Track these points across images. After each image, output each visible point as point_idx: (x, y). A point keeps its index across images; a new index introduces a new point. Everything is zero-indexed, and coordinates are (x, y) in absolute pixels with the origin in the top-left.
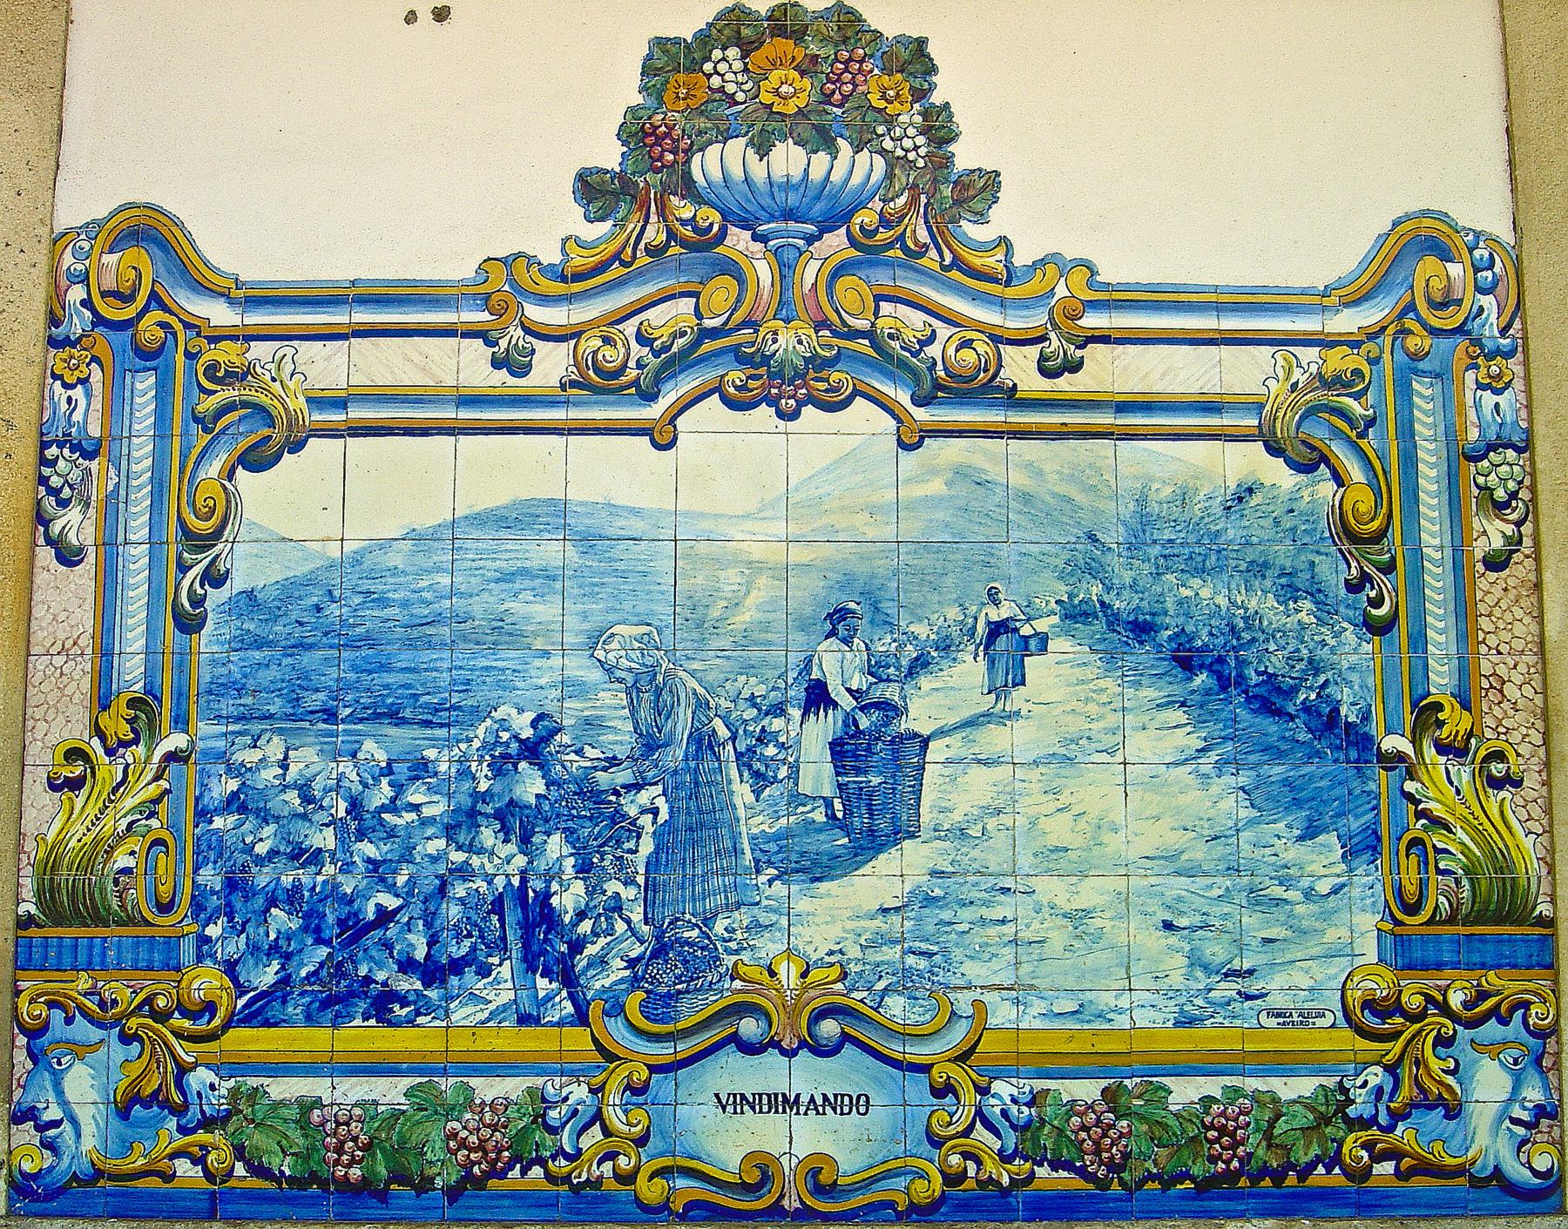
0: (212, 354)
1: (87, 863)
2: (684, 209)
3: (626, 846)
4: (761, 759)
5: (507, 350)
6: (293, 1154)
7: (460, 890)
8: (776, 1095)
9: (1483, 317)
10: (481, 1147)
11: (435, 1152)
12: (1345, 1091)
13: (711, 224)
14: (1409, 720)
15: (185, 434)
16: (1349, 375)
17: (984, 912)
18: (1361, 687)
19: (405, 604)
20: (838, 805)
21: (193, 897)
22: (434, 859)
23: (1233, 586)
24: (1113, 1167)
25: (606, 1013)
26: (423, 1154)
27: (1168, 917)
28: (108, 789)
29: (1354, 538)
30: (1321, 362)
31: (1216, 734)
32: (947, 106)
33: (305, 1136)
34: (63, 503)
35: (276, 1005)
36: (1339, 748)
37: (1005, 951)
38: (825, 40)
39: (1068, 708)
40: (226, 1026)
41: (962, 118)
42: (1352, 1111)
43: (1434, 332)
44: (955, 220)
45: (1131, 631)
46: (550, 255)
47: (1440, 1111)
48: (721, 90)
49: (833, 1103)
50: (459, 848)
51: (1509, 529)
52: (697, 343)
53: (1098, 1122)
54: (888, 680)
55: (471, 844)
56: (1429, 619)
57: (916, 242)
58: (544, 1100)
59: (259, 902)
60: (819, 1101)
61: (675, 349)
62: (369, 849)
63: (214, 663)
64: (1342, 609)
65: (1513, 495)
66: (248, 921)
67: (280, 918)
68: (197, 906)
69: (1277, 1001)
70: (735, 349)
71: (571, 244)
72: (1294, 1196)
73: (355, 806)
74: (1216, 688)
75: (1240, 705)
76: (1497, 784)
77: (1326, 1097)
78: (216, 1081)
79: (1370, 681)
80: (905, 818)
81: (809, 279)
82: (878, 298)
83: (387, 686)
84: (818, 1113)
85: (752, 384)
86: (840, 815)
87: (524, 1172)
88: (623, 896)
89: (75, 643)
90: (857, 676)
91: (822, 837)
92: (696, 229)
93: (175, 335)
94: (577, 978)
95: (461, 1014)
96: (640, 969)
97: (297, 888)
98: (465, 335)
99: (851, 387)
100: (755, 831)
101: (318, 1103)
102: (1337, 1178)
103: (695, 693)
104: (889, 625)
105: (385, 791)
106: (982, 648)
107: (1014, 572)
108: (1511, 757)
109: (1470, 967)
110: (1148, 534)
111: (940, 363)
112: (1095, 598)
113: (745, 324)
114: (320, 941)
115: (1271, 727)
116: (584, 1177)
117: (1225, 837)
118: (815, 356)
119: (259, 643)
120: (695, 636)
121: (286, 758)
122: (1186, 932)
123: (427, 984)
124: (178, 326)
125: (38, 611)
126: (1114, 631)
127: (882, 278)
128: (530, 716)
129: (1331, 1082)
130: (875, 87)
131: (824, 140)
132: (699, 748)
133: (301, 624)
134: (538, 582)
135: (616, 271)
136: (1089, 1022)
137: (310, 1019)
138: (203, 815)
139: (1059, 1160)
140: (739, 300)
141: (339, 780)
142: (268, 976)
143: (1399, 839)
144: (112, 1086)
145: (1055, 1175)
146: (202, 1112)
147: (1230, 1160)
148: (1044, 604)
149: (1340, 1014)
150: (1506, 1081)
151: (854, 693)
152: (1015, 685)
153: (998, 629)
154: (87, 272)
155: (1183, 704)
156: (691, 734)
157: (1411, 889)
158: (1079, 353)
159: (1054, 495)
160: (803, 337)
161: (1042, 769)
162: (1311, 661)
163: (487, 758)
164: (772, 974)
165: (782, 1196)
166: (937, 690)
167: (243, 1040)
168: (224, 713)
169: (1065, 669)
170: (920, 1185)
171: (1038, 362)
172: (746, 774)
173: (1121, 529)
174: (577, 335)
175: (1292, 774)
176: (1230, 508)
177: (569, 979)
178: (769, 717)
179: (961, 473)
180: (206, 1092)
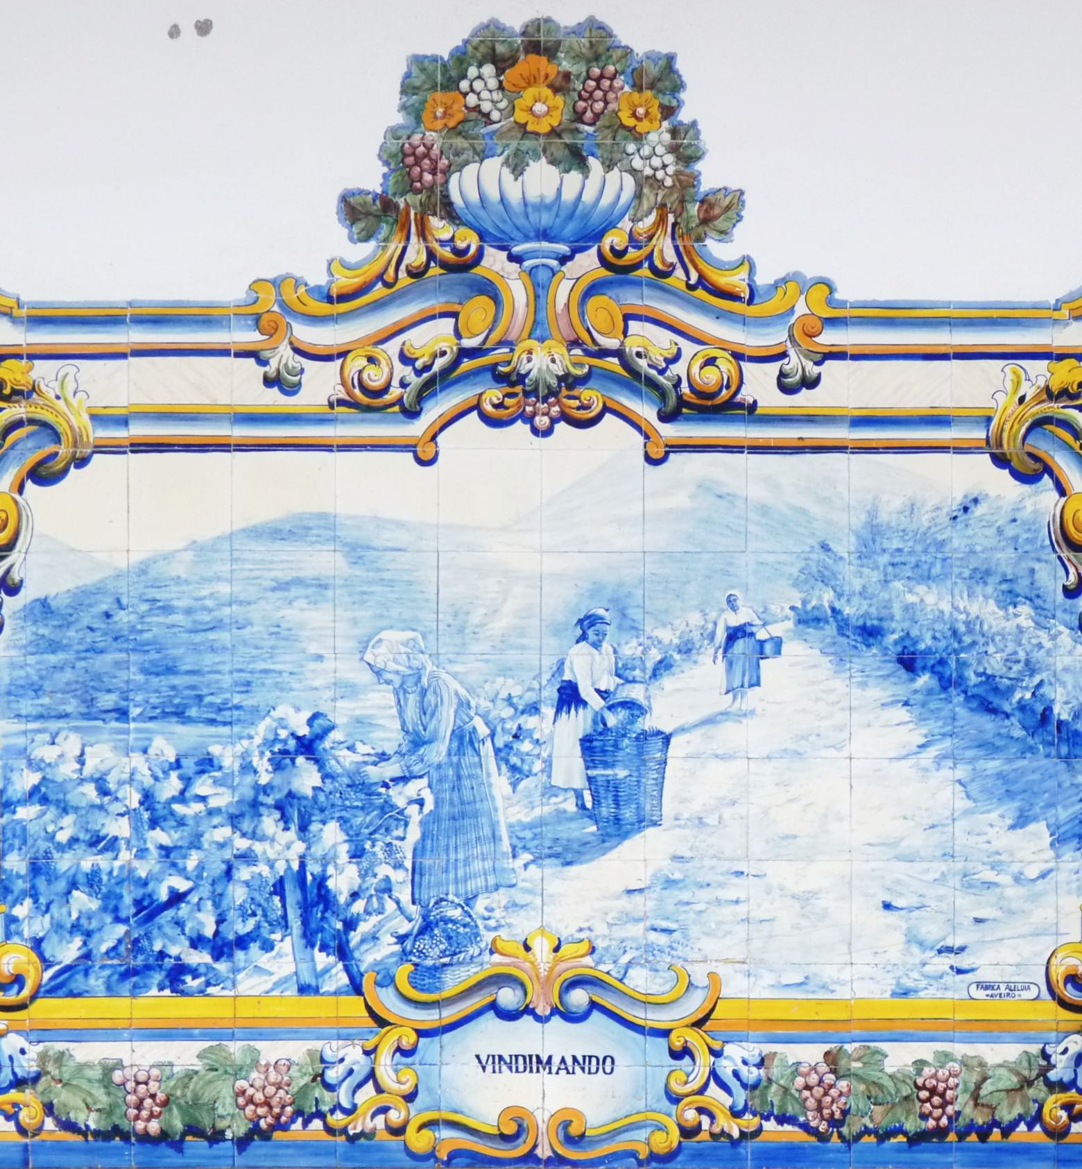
2: (440, 228)
4: (518, 754)
5: (278, 371)
6: (98, 1110)
7: (244, 873)
8: (531, 1057)
10: (267, 1103)
11: (226, 1107)
12: (1045, 1055)
16: (1075, 387)
18: (1074, 687)
19: (188, 611)
22: (222, 846)
23: (956, 591)
25: (378, 984)
26: (214, 1109)
30: (1048, 375)
31: (936, 731)
32: (694, 124)
33: (109, 1094)
35: (80, 977)
36: (1051, 744)
38: (578, 57)
40: (34, 997)
41: (708, 138)
42: (1053, 1075)
44: (699, 239)
45: (859, 635)
46: (318, 278)
48: (477, 108)
49: (583, 1063)
50: (244, 835)
52: (456, 363)
53: (821, 1081)
54: (634, 681)
55: (254, 832)
57: (663, 261)
58: (322, 1060)
59: (61, 885)
60: (569, 1061)
62: (159, 836)
64: (1059, 614)
67: (82, 901)
69: (985, 975)
70: (493, 368)
72: (999, 1150)
73: (147, 798)
75: (959, 704)
77: (1029, 1062)
78: (26, 1045)
80: (648, 807)
82: (627, 318)
83: (173, 688)
84: (568, 1073)
85: (508, 401)
86: (589, 805)
87: (306, 1123)
88: (393, 879)
91: (574, 825)
92: (456, 251)
94: (352, 952)
95: (248, 984)
96: (408, 944)
98: (238, 355)
99: (601, 405)
100: (512, 820)
101: (119, 1065)
103: (457, 694)
104: (635, 629)
105: (173, 785)
106: (721, 651)
110: (878, 543)
113: (502, 343)
114: (118, 920)
115: (988, 724)
116: (358, 1130)
117: (942, 825)
119: (54, 647)
120: (457, 640)
121: (82, 754)
122: (903, 913)
123: (217, 956)
126: (843, 635)
127: (633, 299)
128: (307, 714)
129: (1035, 1049)
131: (576, 159)
132: (461, 744)
133: (91, 629)
134: (311, 590)
135: (379, 291)
136: (813, 992)
137: (110, 991)
139: (784, 1115)
140: (495, 321)
141: (132, 774)
142: (69, 951)
145: (780, 1128)
146: (14, 1074)
148: (778, 611)
149: (1044, 988)
151: (603, 694)
152: (751, 686)
153: (734, 635)
155: (906, 704)
156: (453, 731)
158: (816, 370)
160: (556, 356)
161: (774, 763)
162: (1027, 663)
164: (527, 948)
165: (535, 1146)
166: (679, 690)
167: (49, 1009)
168: (24, 713)
171: (779, 379)
172: (504, 768)
173: (853, 539)
174: (343, 354)
175: (1005, 767)
176: (955, 518)
177: (343, 953)
178: (525, 716)
179: (703, 487)
180: (17, 1056)
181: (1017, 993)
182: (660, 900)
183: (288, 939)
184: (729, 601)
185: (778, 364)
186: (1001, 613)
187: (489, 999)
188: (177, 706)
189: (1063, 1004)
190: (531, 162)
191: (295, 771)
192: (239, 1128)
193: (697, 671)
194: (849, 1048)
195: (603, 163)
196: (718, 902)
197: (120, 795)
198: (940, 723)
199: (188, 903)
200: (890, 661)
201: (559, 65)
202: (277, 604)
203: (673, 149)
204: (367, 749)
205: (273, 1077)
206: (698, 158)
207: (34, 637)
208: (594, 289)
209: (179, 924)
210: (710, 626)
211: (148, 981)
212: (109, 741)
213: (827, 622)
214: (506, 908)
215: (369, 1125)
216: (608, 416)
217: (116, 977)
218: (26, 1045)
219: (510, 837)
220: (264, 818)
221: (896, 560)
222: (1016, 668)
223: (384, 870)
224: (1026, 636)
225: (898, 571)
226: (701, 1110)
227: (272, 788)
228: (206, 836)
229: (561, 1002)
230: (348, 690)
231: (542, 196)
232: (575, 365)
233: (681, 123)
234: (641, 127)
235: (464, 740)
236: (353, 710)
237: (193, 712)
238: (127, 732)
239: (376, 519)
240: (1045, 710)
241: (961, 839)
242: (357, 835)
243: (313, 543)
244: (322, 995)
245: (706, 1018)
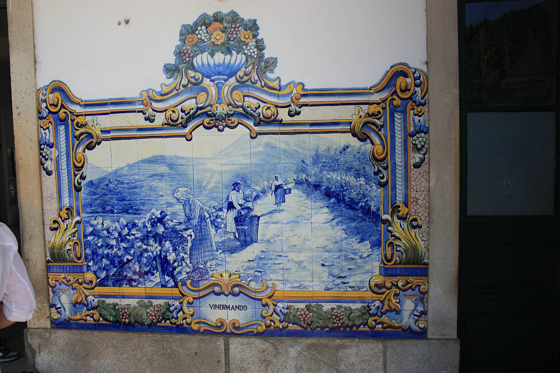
0: (78, 120)
1: (61, 248)
2: (191, 73)
3: (185, 244)
6: (113, 316)
8: (224, 305)
9: (417, 94)
10: (155, 316)
11: (145, 316)
12: (369, 307)
13: (199, 78)
14: (390, 210)
15: (73, 140)
16: (376, 113)
18: (377, 201)
19: (128, 184)
20: (237, 234)
21: (85, 256)
22: (139, 247)
23: (342, 174)
24: (308, 324)
25: (182, 285)
27: (323, 263)
28: (63, 230)
30: (368, 109)
31: (337, 215)
33: (115, 312)
34: (46, 160)
35: (106, 282)
36: (370, 218)
37: (280, 271)
38: (228, 22)
39: (296, 208)
40: (95, 286)
41: (266, 43)
42: (371, 312)
43: (402, 99)
44: (264, 73)
45: (314, 187)
46: (158, 89)
47: (395, 313)
48: (201, 39)
49: (238, 307)
50: (145, 245)
51: (421, 156)
53: (305, 314)
54: (249, 201)
56: (397, 182)
57: (254, 79)
58: (169, 305)
59: (100, 257)
60: (235, 307)
61: (191, 113)
62: (123, 245)
63: (85, 199)
64: (372, 180)
65: (423, 146)
66: (98, 261)
68: (86, 258)
70: (206, 113)
73: (120, 234)
74: (337, 202)
75: (343, 207)
76: (414, 227)
77: (364, 308)
78: (94, 299)
79: (380, 200)
80: (254, 237)
81: (225, 92)
82: (244, 96)
83: (125, 204)
84: (234, 310)
85: (211, 122)
86: (237, 237)
87: (165, 321)
88: (184, 257)
89: (53, 195)
90: (241, 200)
91: (233, 242)
92: (196, 80)
93: (68, 115)
94: (175, 276)
97: (108, 254)
98: (138, 112)
100: (216, 241)
101: (117, 304)
102: (366, 329)
103: (200, 206)
104: (249, 187)
105: (126, 231)
106: (273, 192)
107: (282, 172)
108: (419, 220)
109: (404, 276)
110: (318, 160)
111: (261, 114)
112: (304, 178)
114: (114, 267)
115: (352, 213)
116: (179, 323)
117: (339, 242)
118: (228, 114)
119: (95, 194)
120: (199, 190)
121: (103, 222)
122: (328, 267)
124: (69, 113)
125: (44, 187)
126: (309, 187)
127: (245, 91)
128: (160, 212)
130: (243, 34)
131: (229, 51)
132: (201, 220)
134: (159, 177)
136: (302, 289)
137: (114, 285)
138: (85, 236)
140: (207, 99)
141: (116, 228)
142: (103, 275)
143: (386, 242)
144: (71, 300)
145: (293, 326)
146: (92, 306)
147: (339, 323)
148: (290, 180)
149: (368, 288)
153: (278, 187)
154: (46, 99)
155: (328, 207)
156: (199, 216)
157: (389, 256)
158: (299, 109)
159: (293, 150)
160: (224, 108)
161: (290, 224)
162: (363, 194)
163: (150, 222)
164: (222, 276)
165: (226, 329)
166: (262, 204)
168: (88, 211)
169: (296, 198)
170: (260, 328)
171: (288, 113)
172: (213, 226)
173: (311, 159)
174: (166, 111)
175: (357, 225)
176: (341, 152)
177: (173, 277)
179: (267, 145)
180: (92, 301)
181: (361, 289)
182: (258, 263)
183: (158, 272)
184: (275, 178)
186: (355, 180)
187: (213, 289)
188: (126, 209)
190: (216, 53)
191: (157, 227)
193: (267, 198)
195: (236, 52)
196: (275, 264)
197: (113, 233)
198: (338, 212)
199: (132, 262)
200: (323, 195)
201: (223, 25)
202: (151, 181)
203: (257, 47)
204: (176, 221)
206: (263, 49)
207: (89, 191)
208: (233, 90)
209: (130, 268)
210: (270, 185)
211: (123, 283)
212: (109, 219)
213: (304, 184)
214: (215, 265)
215: (182, 322)
217: (115, 282)
218: (94, 299)
219: (216, 246)
220: (150, 240)
221: (324, 165)
222: (360, 196)
223: (182, 254)
224: (363, 186)
225: (325, 168)
226: (271, 321)
227: (152, 232)
228: (135, 245)
229: (232, 291)
230: (170, 205)
232: (230, 111)
233: (258, 39)
235: (202, 219)
236: (172, 210)
238: (114, 217)
239: (176, 156)
240: (368, 208)
241: (344, 246)
242: (175, 245)
243: (159, 164)
244: (168, 287)
245: (272, 296)
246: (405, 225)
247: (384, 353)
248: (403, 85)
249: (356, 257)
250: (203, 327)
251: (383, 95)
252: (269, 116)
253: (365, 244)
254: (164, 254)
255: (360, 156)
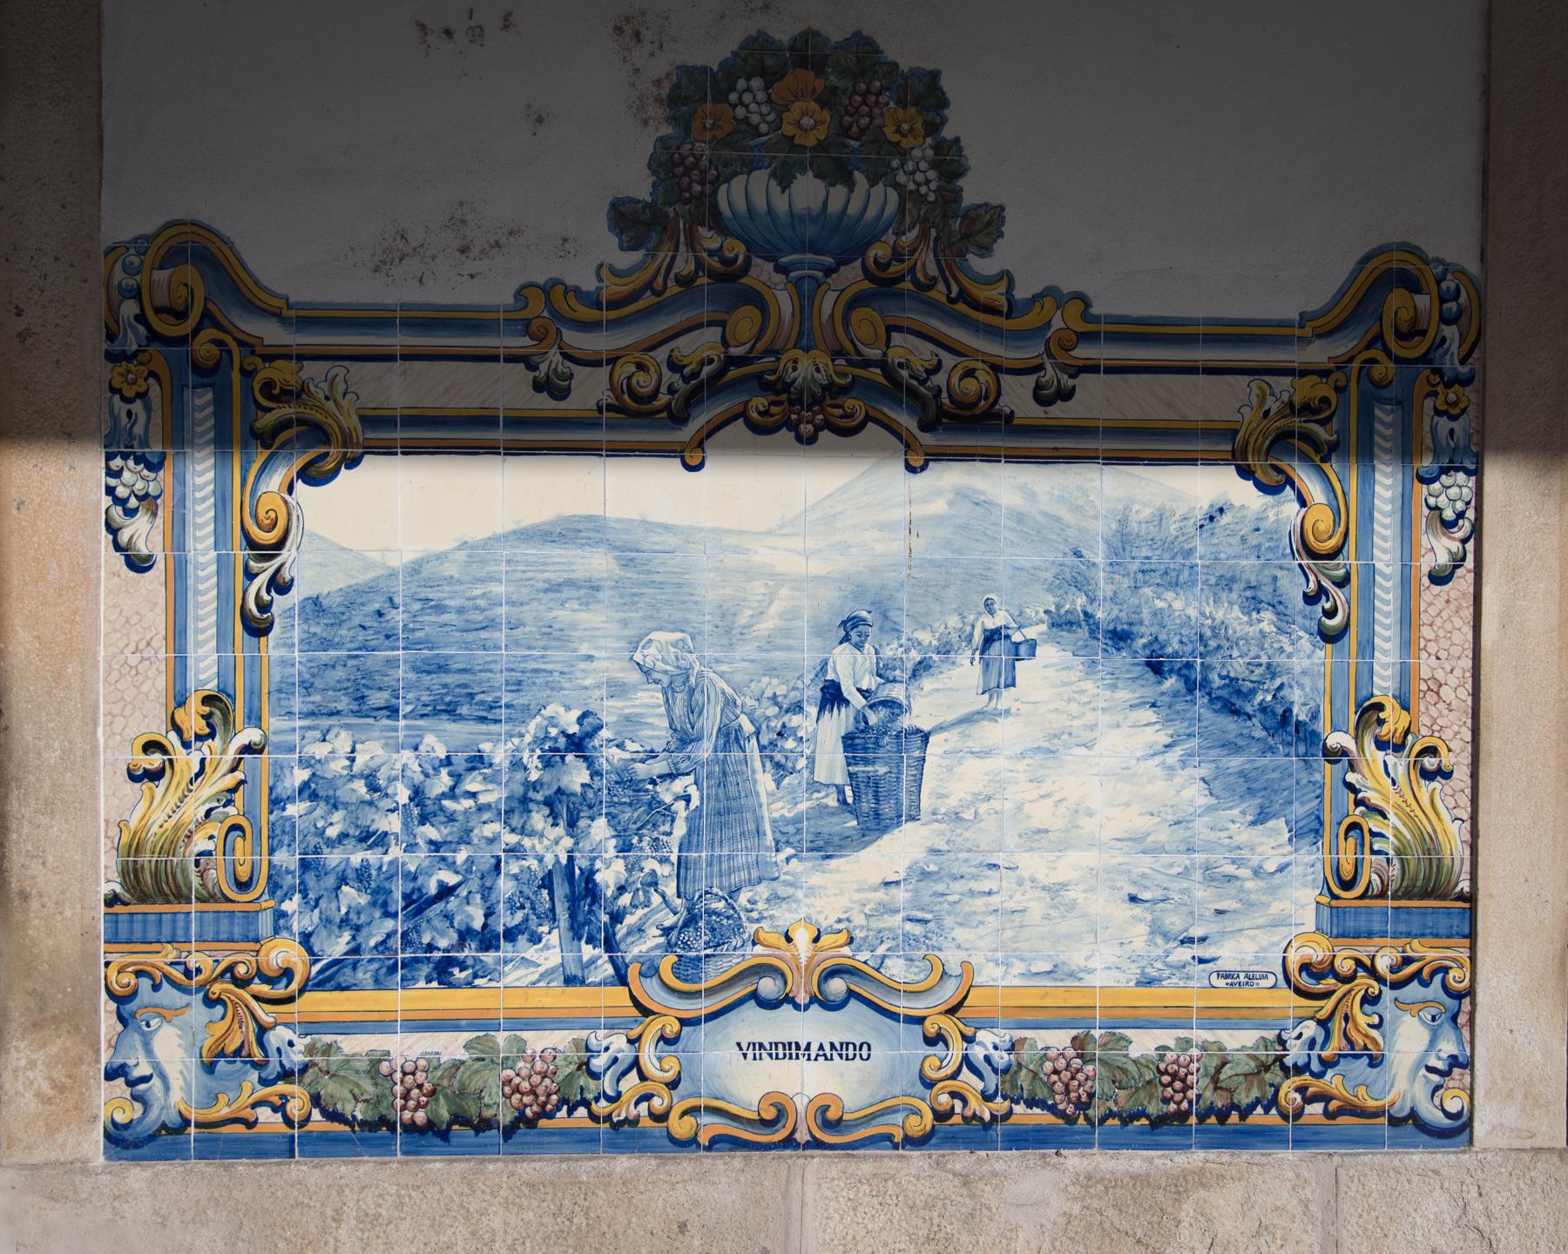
0: (267, 372)
1: (170, 847)
3: (663, 828)
4: (783, 750)
5: (548, 376)
6: (365, 1101)
7: (514, 868)
8: (790, 1044)
9: (1446, 346)
10: (533, 1092)
13: (737, 256)
14: (1353, 718)
17: (973, 885)
19: (461, 611)
20: (848, 792)
21: (270, 877)
22: (491, 841)
26: (480, 1098)
27: (1134, 891)
28: (186, 780)
29: (1313, 555)
31: (1183, 731)
32: (957, 140)
33: (376, 1084)
34: (130, 513)
35: (348, 971)
37: (991, 918)
39: (1052, 707)
40: (302, 991)
41: (973, 154)
43: (1399, 360)
44: (962, 254)
46: (589, 284)
47: (1365, 1060)
48: (746, 120)
49: (842, 1050)
50: (513, 830)
52: (722, 371)
53: (1068, 1065)
54: (895, 681)
55: (523, 827)
57: (925, 274)
58: (588, 1049)
59: (330, 881)
60: (827, 1047)
62: (430, 832)
64: (1299, 619)
65: (1461, 515)
66: (320, 898)
67: (351, 896)
68: (274, 886)
69: (1226, 964)
70: (759, 376)
71: (605, 272)
72: (1236, 1132)
73: (417, 794)
74: (1184, 690)
76: (1427, 775)
78: (295, 1039)
79: (1320, 685)
82: (890, 329)
83: (445, 686)
84: (826, 1059)
85: (774, 409)
86: (850, 800)
87: (570, 1112)
88: (659, 873)
89: (148, 644)
90: (867, 677)
91: (835, 820)
93: (229, 352)
97: (364, 868)
99: (863, 413)
100: (776, 815)
103: (723, 693)
104: (896, 631)
105: (444, 781)
108: (1443, 750)
109: (1396, 936)
110: (1127, 551)
112: (1079, 609)
113: (769, 352)
114: (388, 914)
115: (1230, 725)
116: (622, 1118)
117: (1187, 821)
118: (832, 384)
119: (326, 644)
120: (725, 641)
122: (1148, 905)
124: (233, 345)
128: (576, 713)
129: (1271, 1035)
131: (839, 173)
133: (364, 628)
134: (583, 592)
135: (648, 300)
136: (1062, 980)
137: (379, 984)
138: (277, 803)
139: (1033, 1099)
142: (337, 946)
143: (1339, 824)
144: (198, 1045)
145: (1029, 1111)
146: (282, 1065)
147: (1181, 1102)
148: (1033, 614)
149: (1281, 977)
150: (1424, 1036)
151: (865, 693)
152: (1007, 686)
153: (991, 637)
154: (139, 287)
155: (1153, 705)
156: (720, 729)
158: (1071, 382)
159: (1045, 514)
160: (821, 366)
161: (1028, 761)
163: (538, 752)
164: (789, 939)
165: (794, 1131)
166: (937, 690)
169: (1051, 672)
170: (914, 1120)
172: (768, 764)
174: (613, 361)
175: (1247, 766)
178: (789, 714)
179: (961, 494)
182: (916, 891)
183: (556, 932)
184: (986, 605)
185: (1035, 377)
186: (1245, 618)
188: (449, 704)
189: (1299, 992)
191: (565, 768)
192: (505, 1117)
193: (956, 671)
194: (1097, 1033)
195: (867, 177)
197: (390, 791)
198: (1186, 724)
199: (458, 896)
200: (1138, 664)
201: (826, 79)
202: (550, 605)
203: (934, 165)
205: (539, 1065)
206: (961, 174)
207: (306, 635)
208: (858, 301)
209: (448, 917)
210: (968, 628)
211: (416, 974)
212: (379, 738)
213: (1080, 626)
214: (768, 900)
215: (633, 1112)
216: (871, 426)
217: (384, 970)
218: (295, 1039)
219: (773, 832)
220: (533, 814)
221: (1145, 567)
222: (1258, 671)
224: (1269, 640)
225: (1147, 577)
226: (954, 1095)
227: (542, 784)
228: (476, 831)
230: (618, 689)
231: (809, 208)
233: (944, 139)
234: (905, 143)
235: (730, 737)
236: (623, 708)
237: (464, 710)
238: (396, 730)
239: (644, 522)
240: (1285, 712)
242: (625, 831)
243: (582, 545)
245: (960, 1004)
246: (1398, 764)
247: (1333, 1205)
248: (1405, 315)
249: (1242, 872)
250: (711, 1126)
251: (1341, 347)
252: (972, 399)
253: (1272, 829)
254: (585, 864)
255: (1257, 536)
